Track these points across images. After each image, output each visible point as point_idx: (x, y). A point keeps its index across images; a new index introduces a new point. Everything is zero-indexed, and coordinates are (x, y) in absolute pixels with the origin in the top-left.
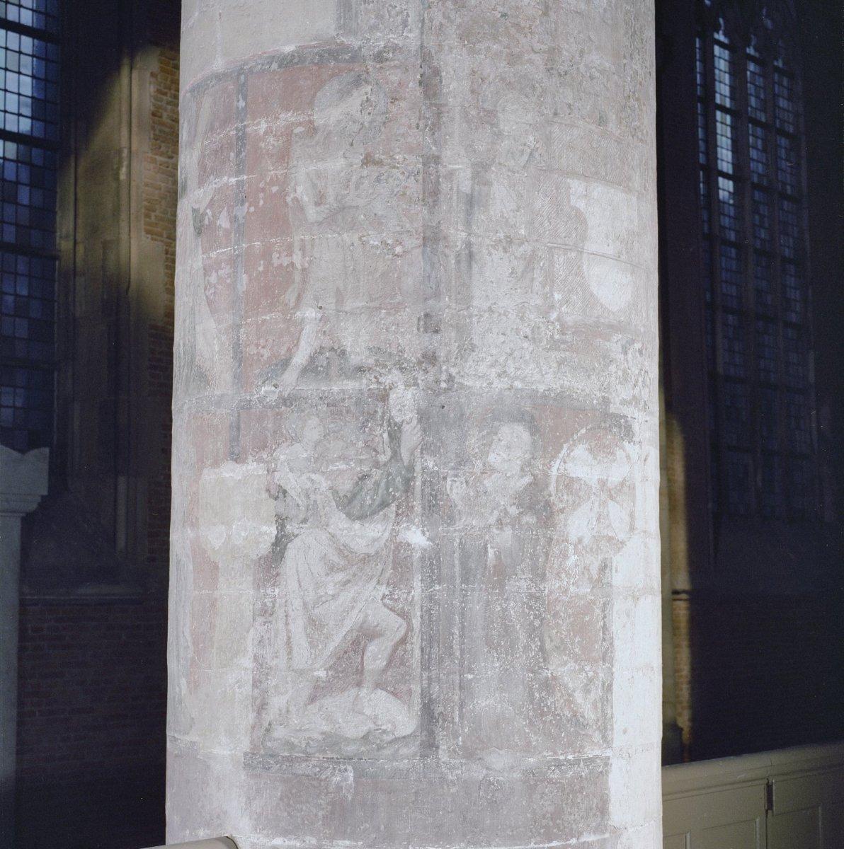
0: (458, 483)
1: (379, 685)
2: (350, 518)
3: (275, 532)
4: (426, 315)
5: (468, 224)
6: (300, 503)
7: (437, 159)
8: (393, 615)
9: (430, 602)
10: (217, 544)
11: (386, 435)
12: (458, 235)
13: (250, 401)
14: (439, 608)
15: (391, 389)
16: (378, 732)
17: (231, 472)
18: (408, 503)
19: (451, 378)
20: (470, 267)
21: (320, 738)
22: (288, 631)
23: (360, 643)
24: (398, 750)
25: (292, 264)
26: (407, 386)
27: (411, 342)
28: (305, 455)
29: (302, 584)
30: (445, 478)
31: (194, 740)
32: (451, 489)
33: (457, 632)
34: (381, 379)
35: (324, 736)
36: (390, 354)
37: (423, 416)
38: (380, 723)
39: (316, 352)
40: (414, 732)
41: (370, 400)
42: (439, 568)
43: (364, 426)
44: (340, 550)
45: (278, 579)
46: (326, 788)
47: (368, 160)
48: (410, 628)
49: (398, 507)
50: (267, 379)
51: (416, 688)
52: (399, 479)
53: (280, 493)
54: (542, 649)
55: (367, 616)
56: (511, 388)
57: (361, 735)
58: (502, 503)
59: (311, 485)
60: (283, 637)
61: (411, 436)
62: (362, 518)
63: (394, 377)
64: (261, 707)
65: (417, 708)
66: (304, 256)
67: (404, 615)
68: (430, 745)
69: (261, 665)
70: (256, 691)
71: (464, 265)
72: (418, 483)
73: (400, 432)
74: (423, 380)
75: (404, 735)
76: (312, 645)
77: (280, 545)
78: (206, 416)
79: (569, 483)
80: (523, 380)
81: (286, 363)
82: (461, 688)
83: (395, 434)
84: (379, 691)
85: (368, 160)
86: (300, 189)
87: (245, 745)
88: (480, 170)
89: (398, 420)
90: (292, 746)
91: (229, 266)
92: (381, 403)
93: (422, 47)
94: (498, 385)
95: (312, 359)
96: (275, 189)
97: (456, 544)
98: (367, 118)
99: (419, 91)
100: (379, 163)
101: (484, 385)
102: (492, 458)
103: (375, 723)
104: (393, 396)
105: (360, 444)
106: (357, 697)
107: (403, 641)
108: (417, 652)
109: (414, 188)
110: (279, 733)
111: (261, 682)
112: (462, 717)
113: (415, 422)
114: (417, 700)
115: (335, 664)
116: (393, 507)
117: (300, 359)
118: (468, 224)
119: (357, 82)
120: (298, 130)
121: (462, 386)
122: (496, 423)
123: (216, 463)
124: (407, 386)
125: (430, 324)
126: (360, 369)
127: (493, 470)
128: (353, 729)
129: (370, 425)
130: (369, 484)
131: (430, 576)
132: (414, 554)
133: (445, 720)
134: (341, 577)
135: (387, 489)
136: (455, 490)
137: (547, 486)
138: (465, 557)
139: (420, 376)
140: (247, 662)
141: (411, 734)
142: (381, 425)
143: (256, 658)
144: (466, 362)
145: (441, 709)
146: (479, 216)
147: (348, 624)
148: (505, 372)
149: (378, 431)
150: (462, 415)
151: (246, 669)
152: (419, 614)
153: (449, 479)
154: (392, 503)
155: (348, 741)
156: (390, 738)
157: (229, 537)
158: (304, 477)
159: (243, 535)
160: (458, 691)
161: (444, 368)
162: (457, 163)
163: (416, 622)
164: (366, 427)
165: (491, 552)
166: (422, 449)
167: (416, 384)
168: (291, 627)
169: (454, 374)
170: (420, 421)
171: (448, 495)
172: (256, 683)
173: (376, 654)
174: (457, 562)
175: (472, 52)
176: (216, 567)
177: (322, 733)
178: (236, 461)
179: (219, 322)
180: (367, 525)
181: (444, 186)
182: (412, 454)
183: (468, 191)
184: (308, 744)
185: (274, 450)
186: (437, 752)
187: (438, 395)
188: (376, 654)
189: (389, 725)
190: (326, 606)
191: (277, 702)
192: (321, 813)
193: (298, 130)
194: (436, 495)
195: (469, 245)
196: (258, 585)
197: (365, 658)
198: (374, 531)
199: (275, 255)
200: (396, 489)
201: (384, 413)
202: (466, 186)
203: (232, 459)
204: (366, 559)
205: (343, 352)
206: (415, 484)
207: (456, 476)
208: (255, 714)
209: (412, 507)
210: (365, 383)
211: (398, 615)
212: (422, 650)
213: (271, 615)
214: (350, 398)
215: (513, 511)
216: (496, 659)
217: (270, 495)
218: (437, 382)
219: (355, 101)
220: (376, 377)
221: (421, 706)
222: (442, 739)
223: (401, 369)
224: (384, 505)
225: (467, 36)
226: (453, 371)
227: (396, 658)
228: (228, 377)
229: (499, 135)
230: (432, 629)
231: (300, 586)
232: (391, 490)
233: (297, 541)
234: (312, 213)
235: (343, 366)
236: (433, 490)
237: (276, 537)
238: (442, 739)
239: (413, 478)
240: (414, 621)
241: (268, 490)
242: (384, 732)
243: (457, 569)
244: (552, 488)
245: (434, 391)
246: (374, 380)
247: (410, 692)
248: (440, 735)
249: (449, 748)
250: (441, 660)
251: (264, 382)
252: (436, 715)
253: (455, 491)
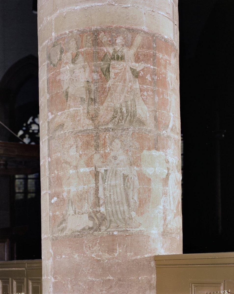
10: (151, 173)
13: (160, 134)
22: (170, 199)
31: (142, 229)
50: (164, 129)
64: (165, 220)
69: (165, 208)
70: (164, 215)
77: (168, 175)
78: (143, 134)
87: (162, 230)
90: (171, 230)
91: (152, 92)
110: (169, 226)
111: (165, 213)
123: (149, 149)
140: (161, 207)
143: (163, 206)
151: (161, 209)
157: (155, 171)
159: (159, 171)
172: (164, 213)
176: (150, 179)
178: (157, 150)
179: (148, 108)
191: (169, 218)
196: (163, 186)
203: (156, 149)
208: (164, 221)
228: (153, 125)
237: (167, 174)
241: (165, 160)
251: (164, 130)
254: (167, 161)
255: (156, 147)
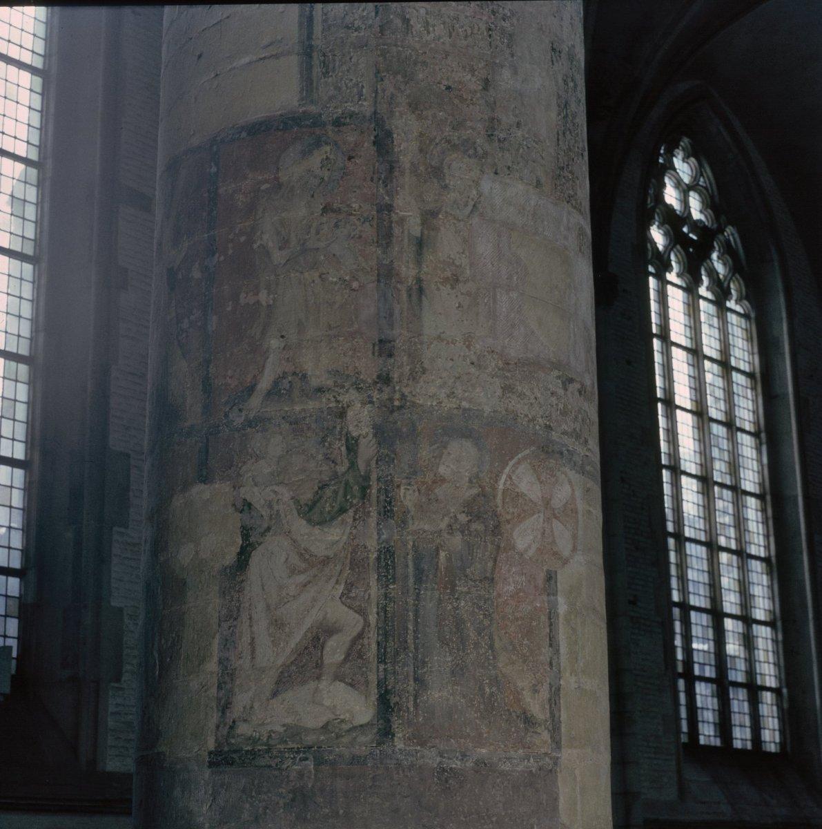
0: (411, 492)
1: (338, 677)
2: (311, 524)
3: (241, 542)
4: (381, 341)
5: (419, 263)
6: (264, 513)
7: (390, 208)
8: (351, 612)
9: (386, 599)
11: (343, 449)
12: (407, 271)
14: (394, 605)
15: (348, 406)
16: (337, 721)
17: (200, 492)
18: (364, 508)
19: (403, 396)
20: (420, 300)
21: (282, 730)
22: (252, 633)
23: (319, 640)
24: (357, 736)
25: (258, 302)
26: (363, 404)
27: (368, 366)
28: (269, 470)
29: (265, 588)
30: (398, 486)
32: (405, 497)
33: (411, 628)
34: (339, 398)
35: (285, 728)
36: (348, 376)
37: (379, 431)
38: (338, 713)
39: (280, 377)
40: (371, 720)
41: (329, 417)
42: (394, 568)
43: (324, 440)
44: (302, 554)
45: (243, 585)
46: (288, 777)
47: (326, 209)
48: (367, 624)
49: (356, 512)
50: (234, 405)
51: (373, 678)
52: (356, 488)
53: (248, 506)
54: (491, 647)
55: (326, 613)
56: (458, 408)
57: (321, 724)
58: (452, 510)
59: (274, 496)
60: (246, 639)
61: (367, 449)
62: (322, 523)
63: (352, 396)
64: (225, 707)
65: (374, 698)
66: (269, 294)
67: (362, 612)
68: (386, 733)
71: (415, 298)
72: (374, 491)
73: (357, 445)
74: (378, 399)
75: (361, 723)
76: (275, 643)
79: (514, 496)
80: (470, 401)
81: (251, 389)
82: (416, 680)
83: (352, 446)
84: (338, 683)
85: (326, 209)
86: (265, 237)
87: (211, 745)
88: (429, 217)
89: (355, 434)
92: (339, 420)
93: (375, 113)
94: (448, 405)
95: (276, 383)
96: (243, 239)
97: (410, 547)
98: (326, 174)
99: (373, 149)
100: (338, 211)
101: (434, 404)
102: (442, 470)
103: (333, 713)
104: (350, 414)
105: (320, 457)
106: (317, 690)
107: (360, 636)
108: (374, 646)
109: (369, 231)
110: (243, 729)
112: (416, 705)
113: (371, 436)
114: (374, 691)
115: (296, 660)
116: (351, 513)
117: (265, 384)
118: (419, 263)
119: (318, 144)
120: (266, 186)
121: (414, 404)
122: (446, 439)
123: (186, 486)
124: (363, 404)
125: (385, 347)
126: (320, 390)
127: (443, 480)
128: (312, 719)
129: (329, 440)
130: (328, 492)
131: (385, 576)
132: (370, 556)
133: (400, 710)
134: (302, 578)
135: (345, 496)
136: (407, 497)
137: (495, 497)
138: (418, 559)
139: (376, 395)
140: (212, 666)
141: (368, 723)
142: (340, 440)
143: (220, 662)
144: (418, 382)
145: (397, 699)
146: (429, 257)
147: (308, 623)
148: (453, 393)
149: (337, 444)
150: (414, 430)
152: (375, 610)
153: (402, 488)
154: (350, 508)
155: (307, 731)
156: (345, 727)
157: (197, 553)
158: (268, 489)
160: (412, 682)
161: (397, 388)
162: (408, 210)
163: (373, 619)
164: (325, 441)
165: (442, 554)
166: (377, 461)
167: (371, 402)
168: (255, 628)
169: (406, 394)
170: (375, 435)
171: (401, 502)
173: (334, 652)
174: (410, 564)
175: (420, 117)
177: (284, 725)
178: (204, 482)
180: (326, 530)
181: (396, 231)
182: (368, 464)
183: (419, 235)
184: (270, 737)
185: (240, 468)
186: (393, 740)
187: (392, 412)
188: (334, 652)
189: (348, 715)
190: (287, 606)
191: (241, 700)
192: (281, 802)
193: (266, 186)
194: (391, 502)
195: (419, 280)
197: (325, 652)
198: (333, 535)
199: (242, 295)
200: (353, 497)
201: (341, 428)
202: (416, 231)
204: (326, 561)
205: (304, 376)
206: (371, 492)
207: (409, 484)
208: (220, 714)
209: (369, 512)
210: (327, 402)
211: (356, 611)
212: (378, 644)
213: (236, 619)
214: (311, 416)
215: (463, 518)
216: (448, 654)
217: (236, 510)
218: (391, 400)
219: (316, 160)
220: (334, 397)
221: (377, 696)
222: (398, 727)
223: (358, 389)
224: (342, 510)
225: (414, 106)
226: (406, 391)
227: (355, 651)
229: (446, 187)
230: (387, 625)
231: (263, 589)
232: (348, 497)
233: (260, 549)
234: (278, 257)
235: (304, 387)
236: (387, 497)
237: (242, 547)
238: (398, 727)
239: (369, 487)
240: (370, 617)
241: (234, 505)
242: (342, 721)
243: (411, 569)
244: (499, 496)
245: (389, 408)
246: (333, 399)
247: (367, 683)
248: (396, 723)
249: (405, 735)
250: (397, 653)
252: (392, 705)
253: (408, 497)
254: (239, 505)
255: (202, 476)
